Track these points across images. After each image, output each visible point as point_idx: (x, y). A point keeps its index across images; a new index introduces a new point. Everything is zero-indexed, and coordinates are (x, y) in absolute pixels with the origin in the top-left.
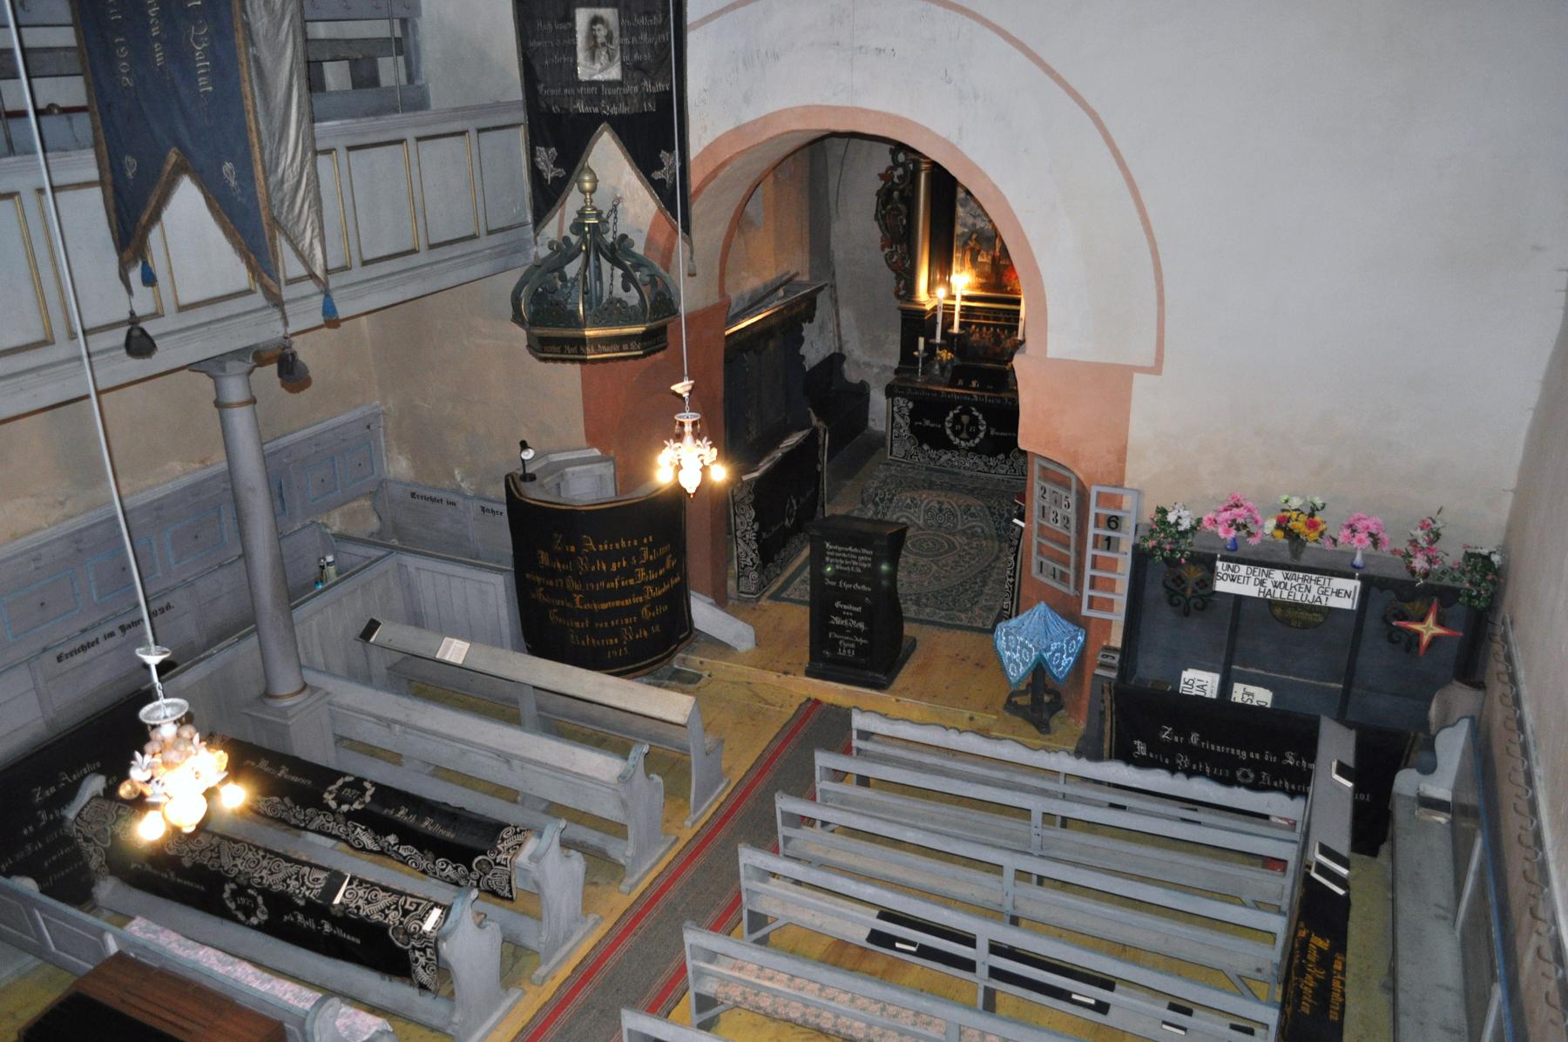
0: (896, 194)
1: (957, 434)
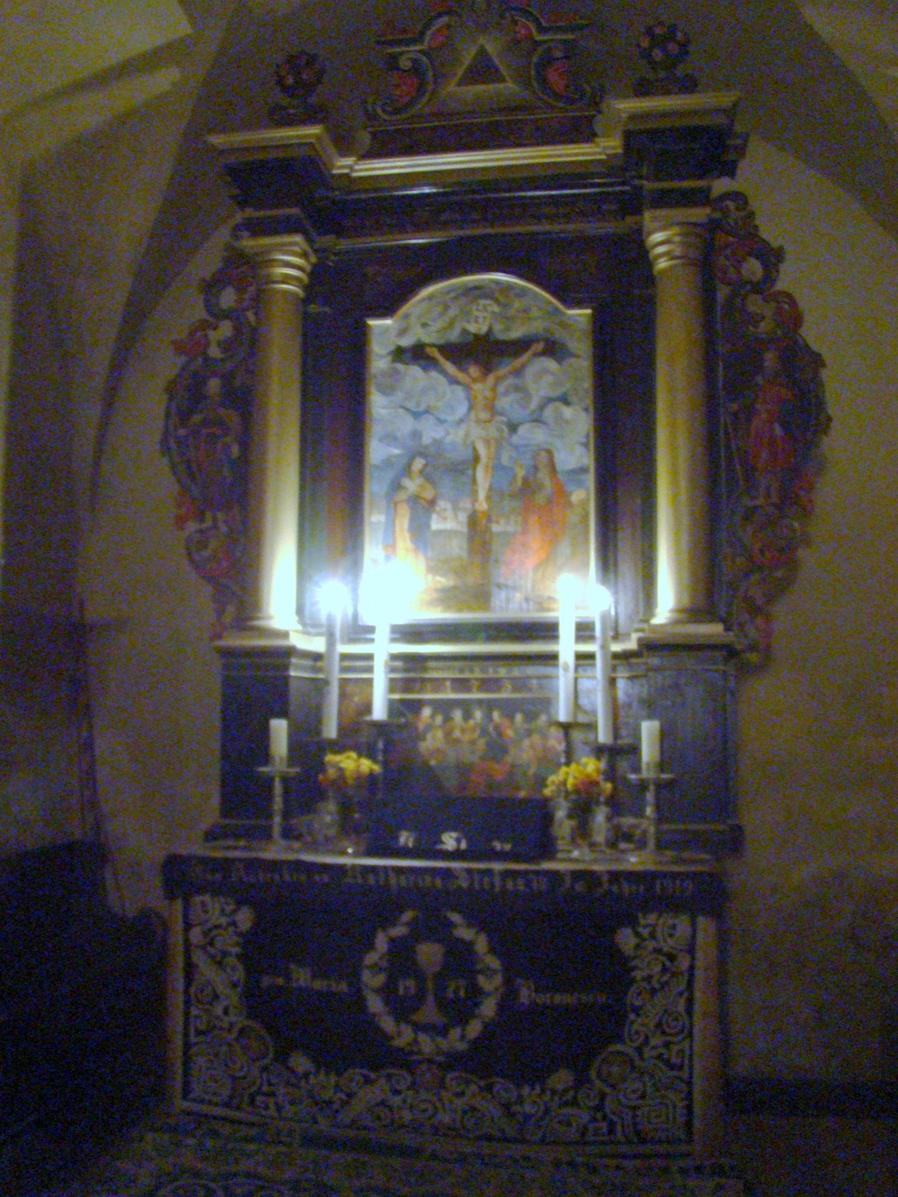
0: (214, 385)
1: (401, 1009)
